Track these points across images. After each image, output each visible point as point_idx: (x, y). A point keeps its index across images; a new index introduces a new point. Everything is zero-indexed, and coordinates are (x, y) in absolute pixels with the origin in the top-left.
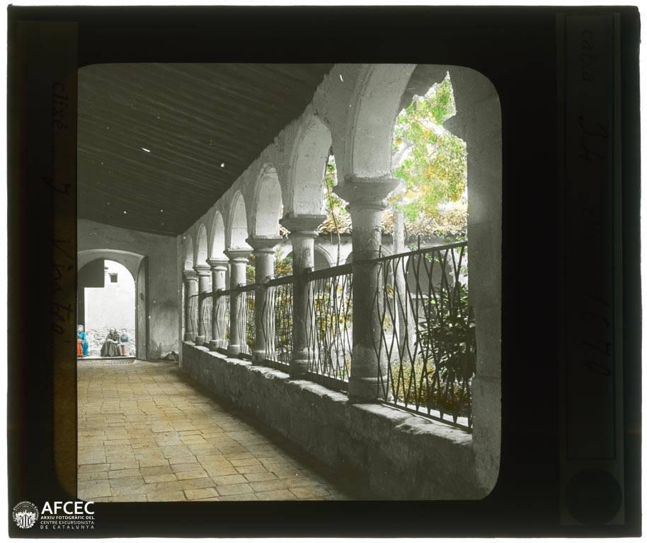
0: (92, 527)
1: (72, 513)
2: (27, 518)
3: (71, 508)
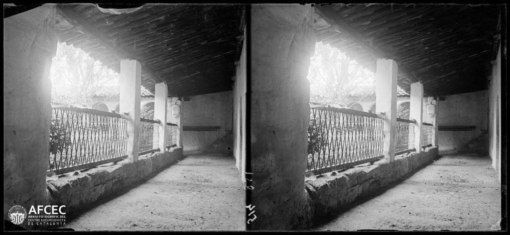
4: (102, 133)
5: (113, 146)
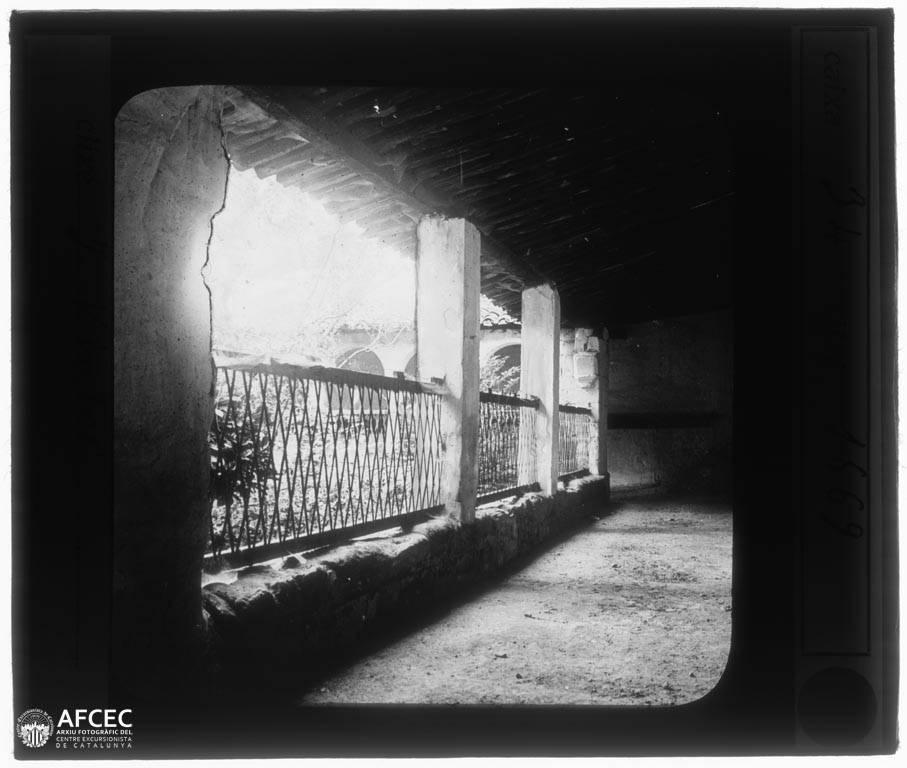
0: (129, 745)
1: (100, 726)
2: (38, 732)
3: (99, 718)
4: (367, 441)
5: (400, 477)
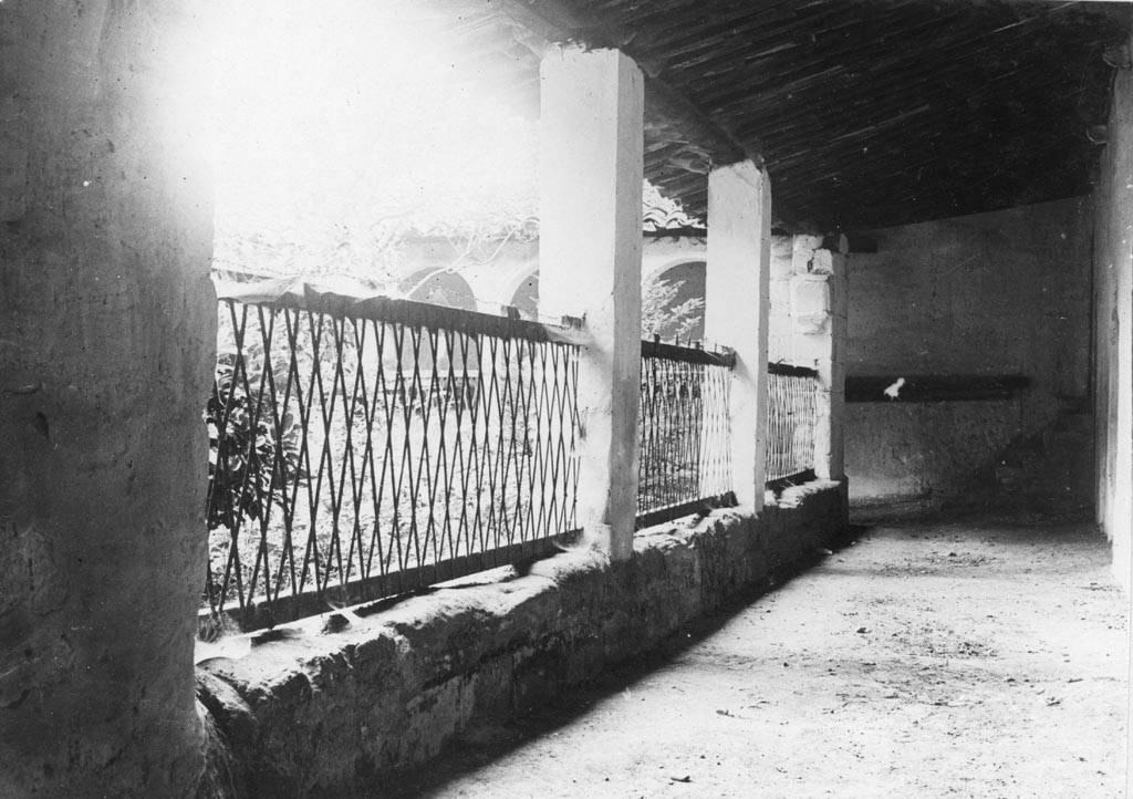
4: (459, 418)
